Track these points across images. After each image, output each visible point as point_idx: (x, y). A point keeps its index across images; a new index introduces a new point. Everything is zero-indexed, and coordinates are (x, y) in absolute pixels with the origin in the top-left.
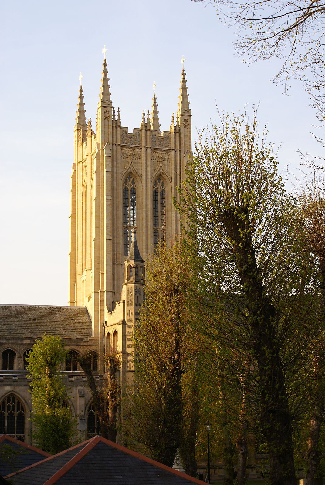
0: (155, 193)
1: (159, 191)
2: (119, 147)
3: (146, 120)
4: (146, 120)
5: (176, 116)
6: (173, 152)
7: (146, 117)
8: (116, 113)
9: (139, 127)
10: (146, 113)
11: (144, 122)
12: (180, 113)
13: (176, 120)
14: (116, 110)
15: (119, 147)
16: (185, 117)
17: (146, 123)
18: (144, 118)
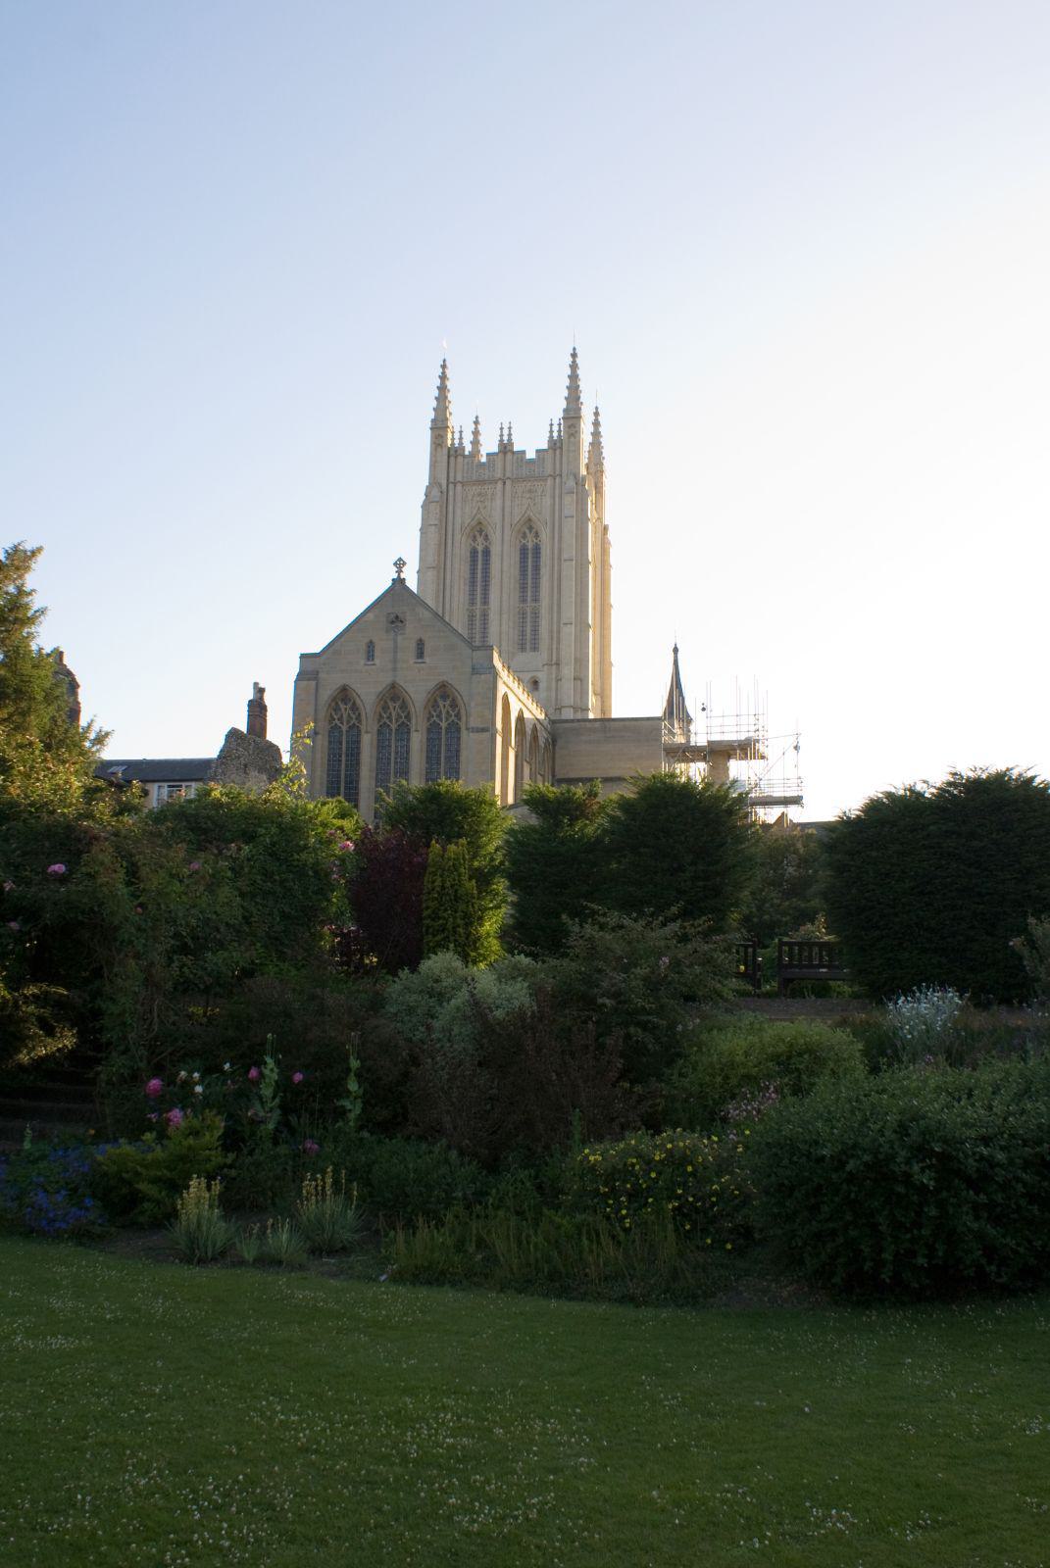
0: (524, 550)
1: (530, 545)
2: (459, 487)
3: (505, 438)
4: (505, 438)
5: (556, 422)
6: (550, 481)
7: (506, 432)
8: (457, 436)
9: (495, 449)
10: (505, 427)
11: (501, 441)
12: (561, 415)
13: (555, 428)
14: (457, 430)
15: (459, 487)
16: (570, 422)
17: (505, 442)
18: (501, 435)
